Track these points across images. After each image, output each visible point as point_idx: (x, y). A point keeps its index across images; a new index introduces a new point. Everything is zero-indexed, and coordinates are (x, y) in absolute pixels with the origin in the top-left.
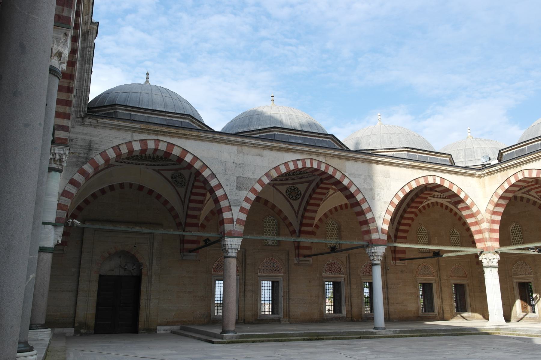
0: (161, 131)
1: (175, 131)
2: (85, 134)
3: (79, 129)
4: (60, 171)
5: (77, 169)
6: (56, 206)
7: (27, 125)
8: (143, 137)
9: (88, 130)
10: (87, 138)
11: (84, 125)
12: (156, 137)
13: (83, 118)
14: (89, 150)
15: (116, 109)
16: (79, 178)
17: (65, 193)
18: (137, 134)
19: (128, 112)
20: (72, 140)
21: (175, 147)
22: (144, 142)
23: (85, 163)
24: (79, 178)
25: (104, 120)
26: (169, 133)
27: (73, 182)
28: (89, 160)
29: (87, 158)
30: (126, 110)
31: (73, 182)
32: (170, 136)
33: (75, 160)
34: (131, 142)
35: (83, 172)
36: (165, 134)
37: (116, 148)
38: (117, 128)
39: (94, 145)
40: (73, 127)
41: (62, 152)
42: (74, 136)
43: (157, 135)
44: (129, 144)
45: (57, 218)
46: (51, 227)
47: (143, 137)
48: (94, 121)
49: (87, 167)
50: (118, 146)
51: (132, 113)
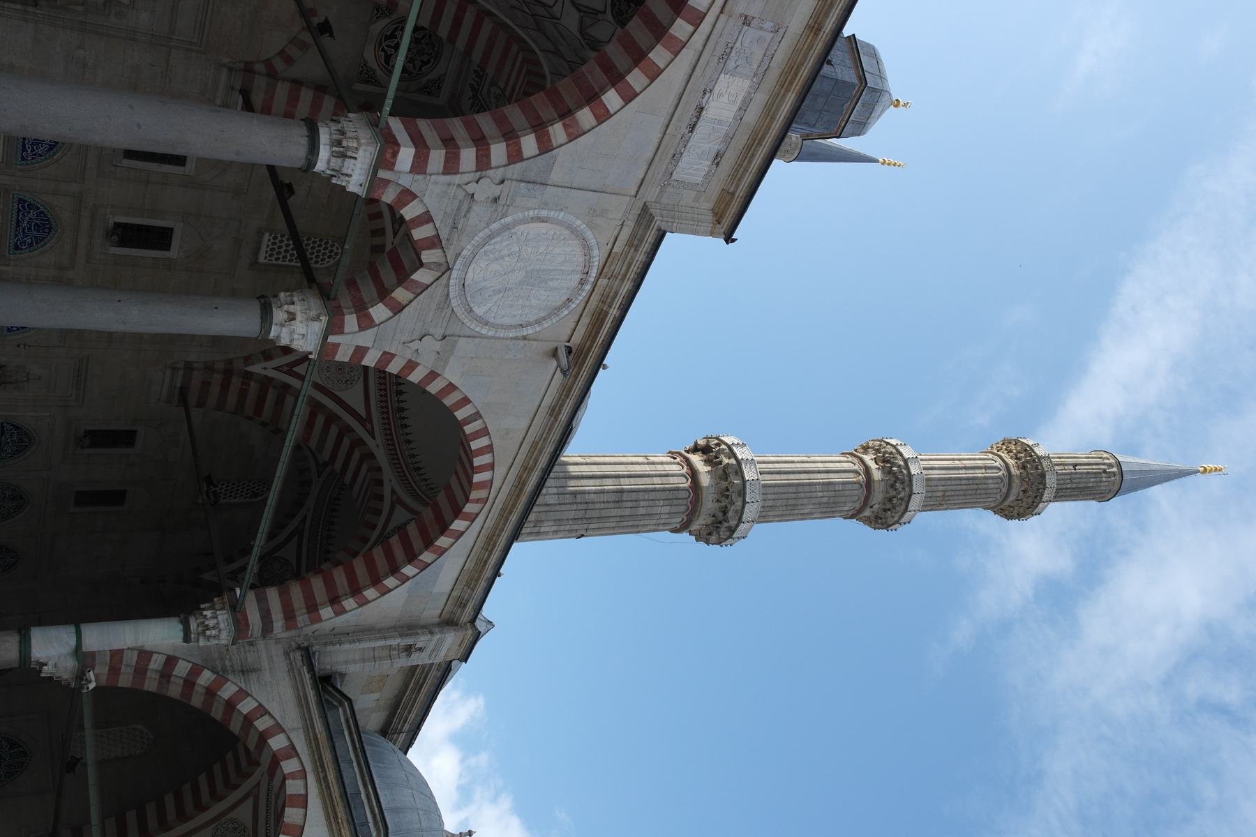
0: (324, 770)
1: (331, 777)
2: (270, 658)
3: (277, 651)
4: (187, 639)
5: (199, 662)
6: (116, 646)
7: (131, 106)
8: (301, 746)
9: (281, 664)
10: (265, 665)
11: (287, 654)
12: (309, 768)
13: (299, 648)
14: (243, 672)
15: (341, 704)
16: (182, 668)
17: (145, 655)
18: (302, 737)
19: (344, 726)
20: (251, 644)
21: (302, 811)
22: (292, 752)
23: (214, 671)
24: (182, 668)
25: (307, 676)
26: (328, 787)
27: (171, 661)
28: (222, 678)
29: (225, 670)
30: (347, 721)
31: (171, 661)
32: (321, 793)
33: (216, 655)
34: (283, 731)
35: (196, 671)
36: (323, 781)
37: (262, 711)
38: (302, 702)
39: (253, 677)
40: (278, 641)
41: (222, 626)
42: (261, 644)
43: (315, 769)
44: (279, 728)
45: (92, 654)
46: (73, 642)
47: (301, 746)
48: (300, 663)
49: (206, 678)
50: (267, 712)
51: (346, 733)
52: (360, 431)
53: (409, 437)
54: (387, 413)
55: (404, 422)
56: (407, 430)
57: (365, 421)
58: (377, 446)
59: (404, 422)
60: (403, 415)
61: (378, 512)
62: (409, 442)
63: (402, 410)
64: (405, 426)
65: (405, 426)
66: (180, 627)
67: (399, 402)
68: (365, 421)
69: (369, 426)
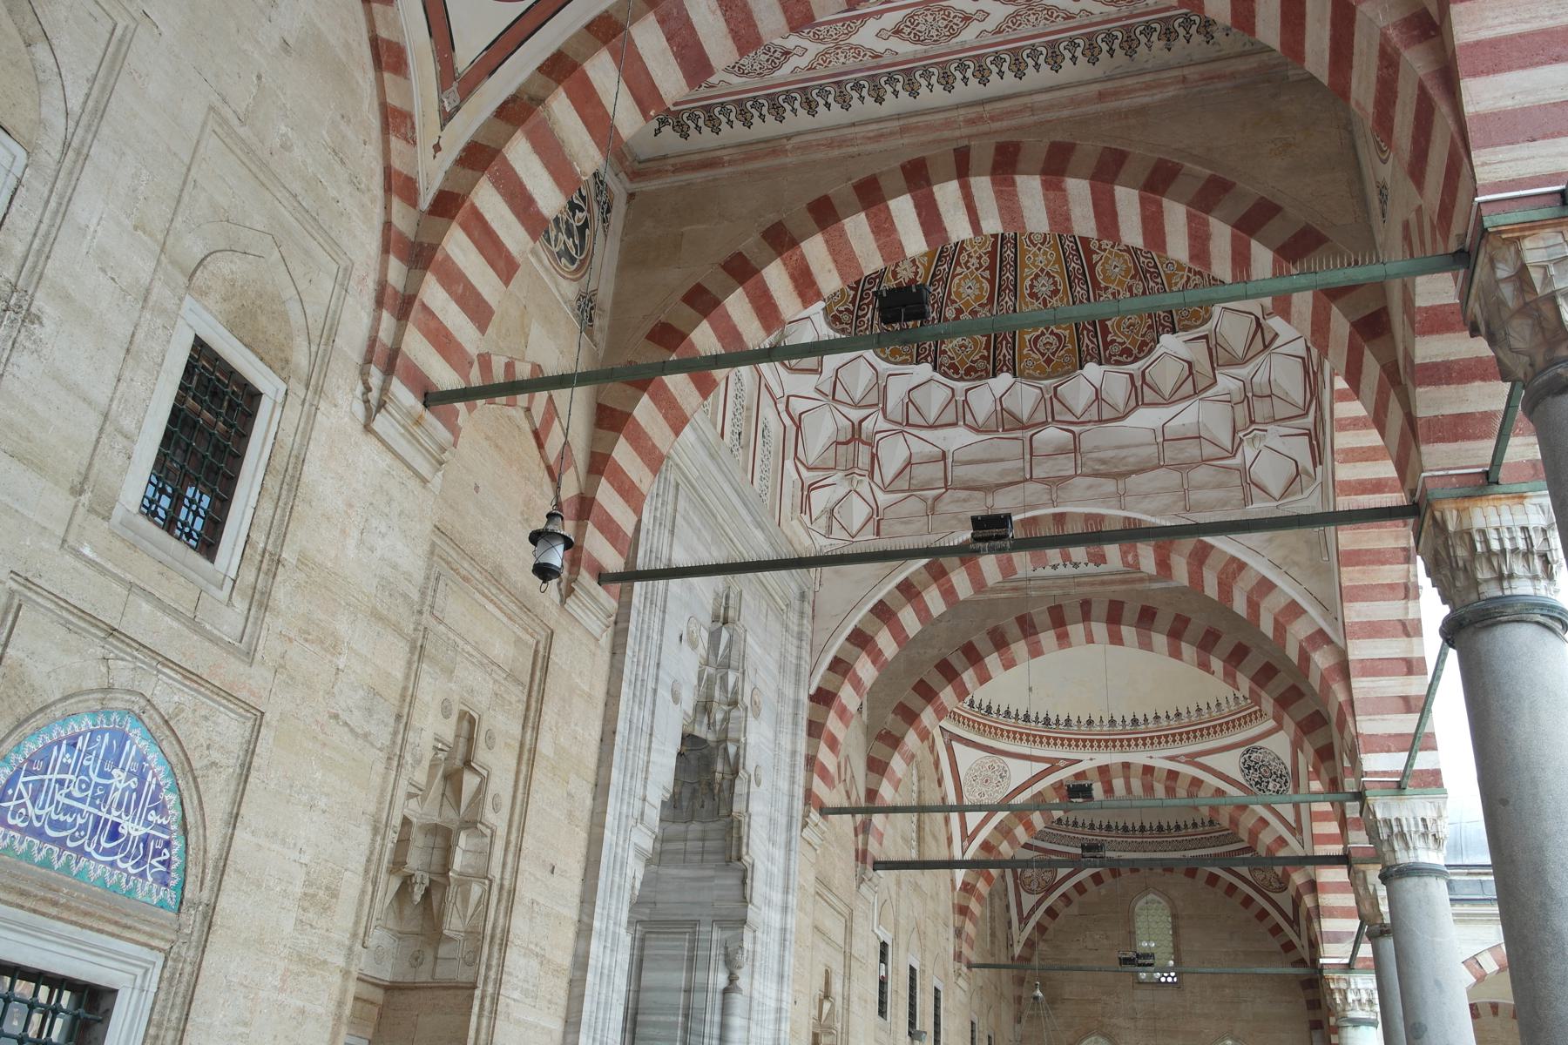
52: (1065, 774)
53: (1084, 720)
54: (1048, 738)
55: (1062, 721)
56: (1074, 721)
57: (1054, 766)
58: (1090, 760)
59: (1062, 721)
60: (1053, 720)
61: (1196, 783)
62: (1090, 722)
63: (1047, 721)
64: (1068, 721)
65: (1068, 721)
66: (1363, 1028)
67: (1037, 721)
68: (1054, 766)
69: (1062, 764)
